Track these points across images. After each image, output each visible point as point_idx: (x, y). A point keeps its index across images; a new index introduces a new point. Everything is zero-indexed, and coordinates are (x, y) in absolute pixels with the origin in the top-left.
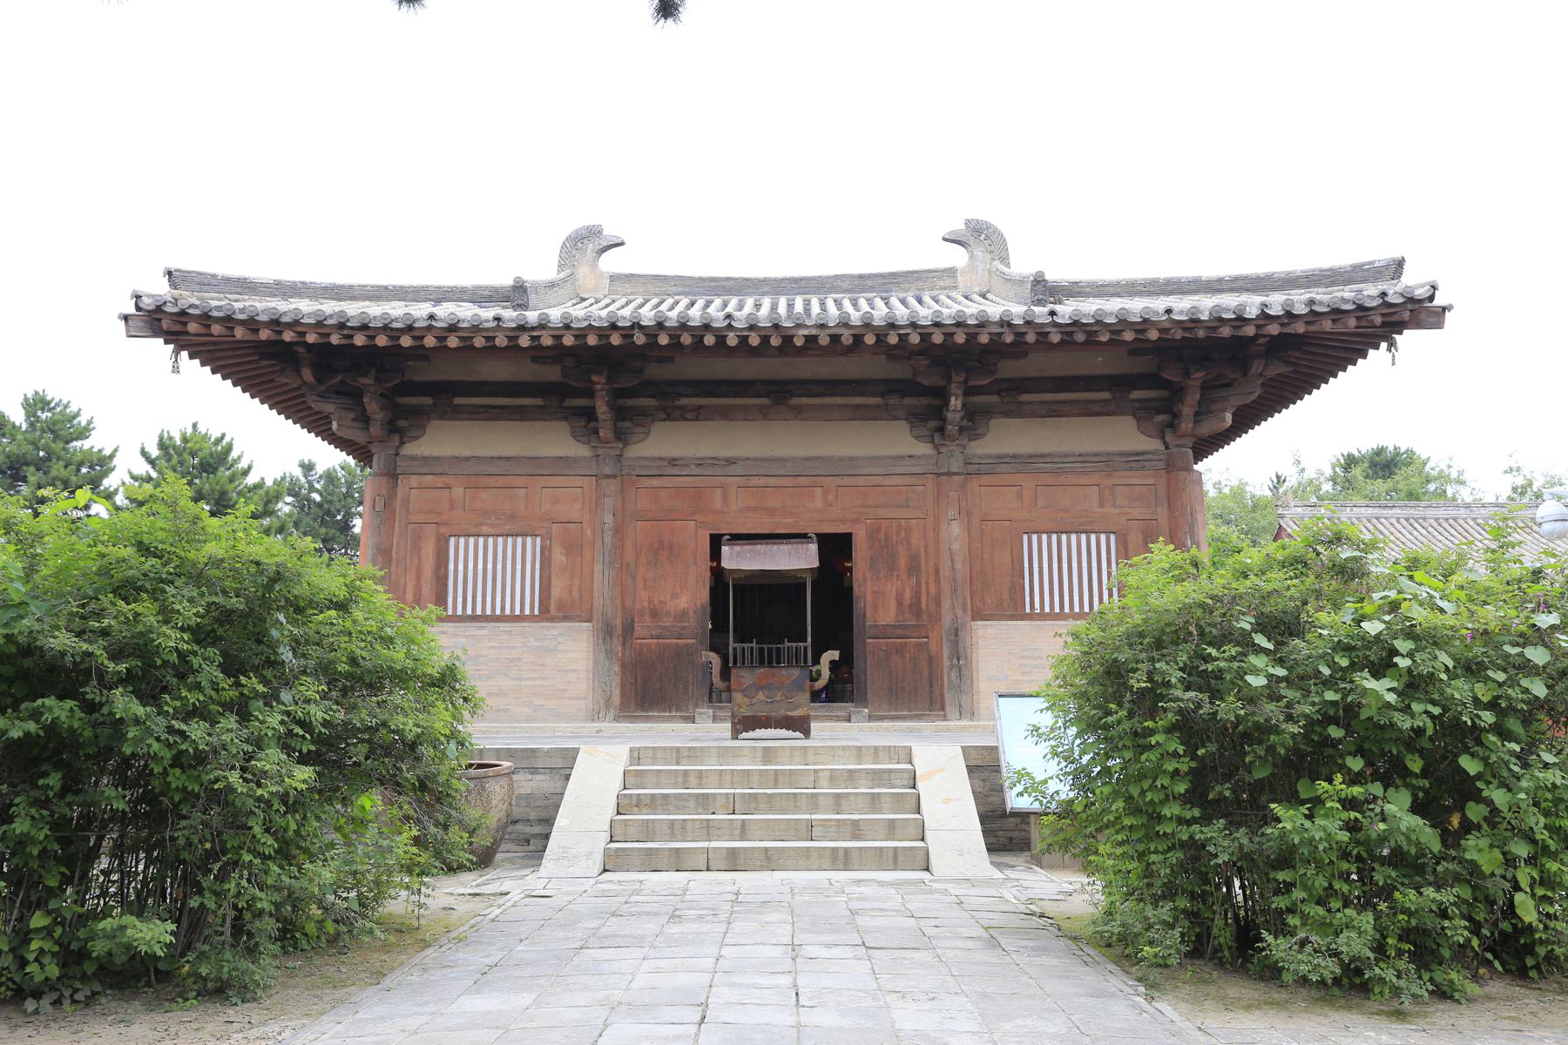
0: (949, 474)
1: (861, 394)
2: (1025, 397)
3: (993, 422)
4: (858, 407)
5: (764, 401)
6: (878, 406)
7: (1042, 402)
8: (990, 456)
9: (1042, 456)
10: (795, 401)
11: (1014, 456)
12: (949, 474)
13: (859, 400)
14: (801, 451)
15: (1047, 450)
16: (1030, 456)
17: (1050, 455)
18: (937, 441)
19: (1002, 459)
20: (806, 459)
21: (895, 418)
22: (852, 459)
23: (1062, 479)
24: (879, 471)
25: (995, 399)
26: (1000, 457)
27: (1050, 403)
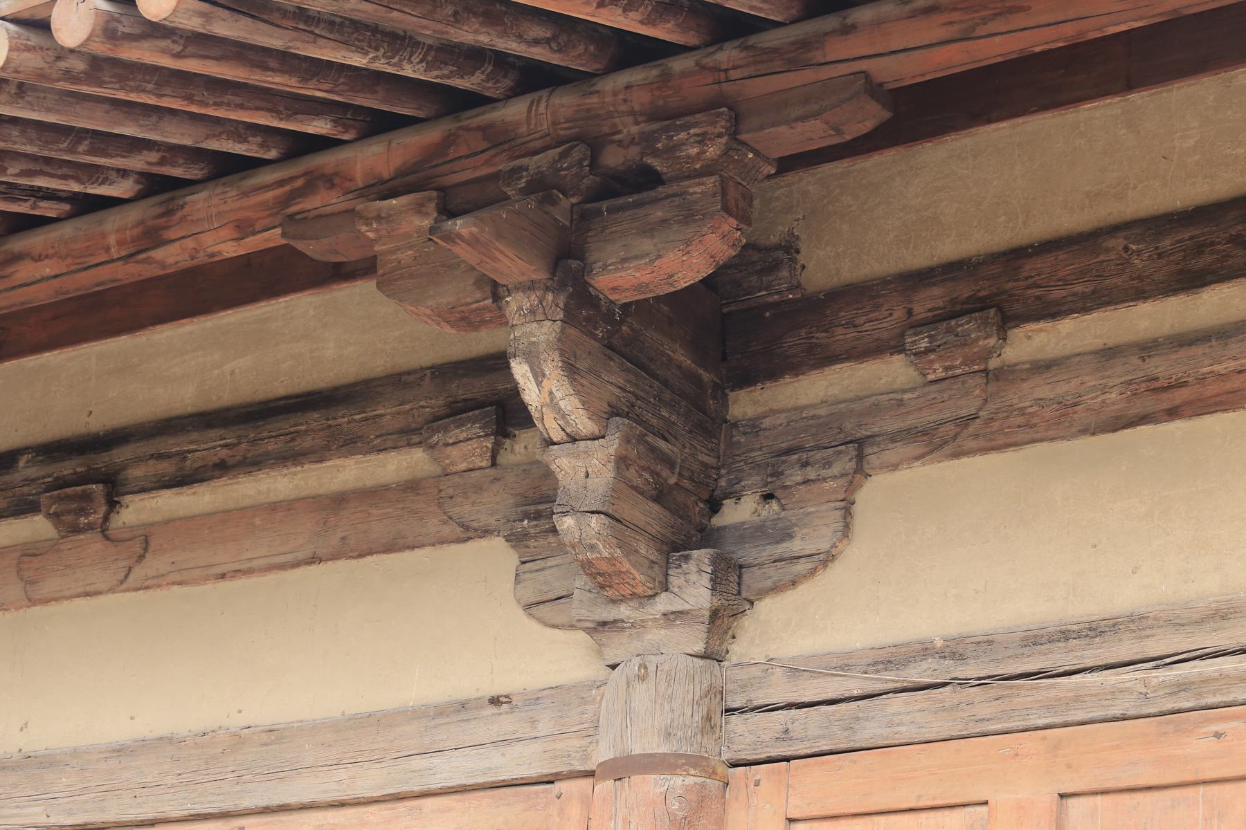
0: (621, 769)
1: (351, 444)
2: (1031, 342)
3: (876, 492)
4: (339, 501)
5: (37, 527)
6: (412, 487)
7: (1109, 354)
8: (843, 664)
9: (1094, 630)
10: (138, 510)
11: (954, 650)
12: (621, 769)
13: (347, 472)
14: (119, 730)
15: (1123, 596)
16: (1033, 640)
17: (1136, 623)
18: (586, 606)
19: (904, 673)
20: (120, 751)
21: (470, 533)
22: (275, 734)
23: (1197, 748)
24: (370, 781)
25: (893, 372)
26: (890, 659)
27: (1147, 348)
